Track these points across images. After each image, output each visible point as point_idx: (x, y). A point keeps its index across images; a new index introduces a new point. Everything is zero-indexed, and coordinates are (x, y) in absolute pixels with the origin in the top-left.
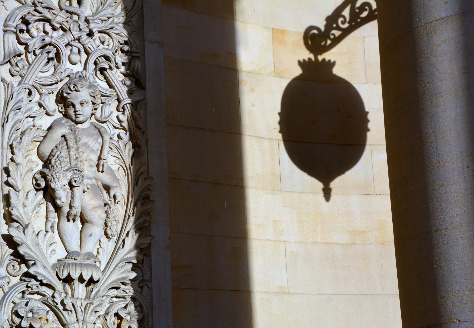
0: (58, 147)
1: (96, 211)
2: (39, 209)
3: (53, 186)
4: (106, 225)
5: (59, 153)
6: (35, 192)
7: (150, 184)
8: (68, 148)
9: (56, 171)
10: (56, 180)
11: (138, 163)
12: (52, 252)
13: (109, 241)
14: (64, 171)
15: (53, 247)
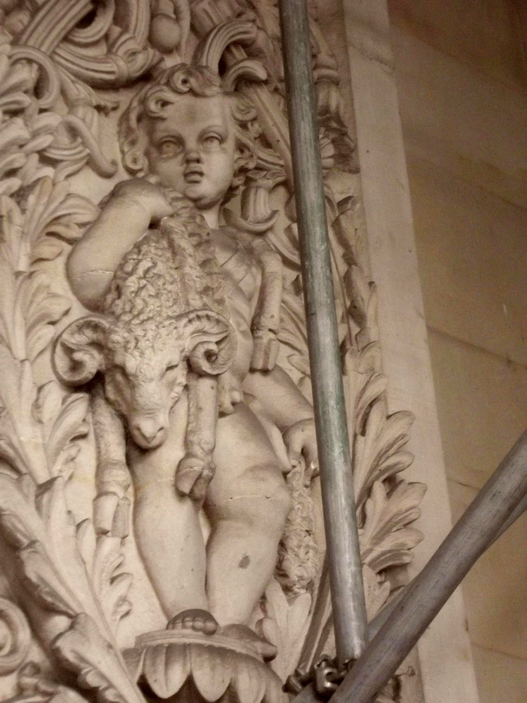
0: (144, 248)
1: (263, 480)
2: (73, 452)
3: (131, 363)
4: (282, 545)
5: (146, 264)
6: (64, 393)
7: (403, 436)
8: (174, 253)
9: (143, 317)
10: (143, 344)
11: (361, 370)
12: (118, 605)
13: (290, 601)
14: (169, 317)
15: (121, 588)
